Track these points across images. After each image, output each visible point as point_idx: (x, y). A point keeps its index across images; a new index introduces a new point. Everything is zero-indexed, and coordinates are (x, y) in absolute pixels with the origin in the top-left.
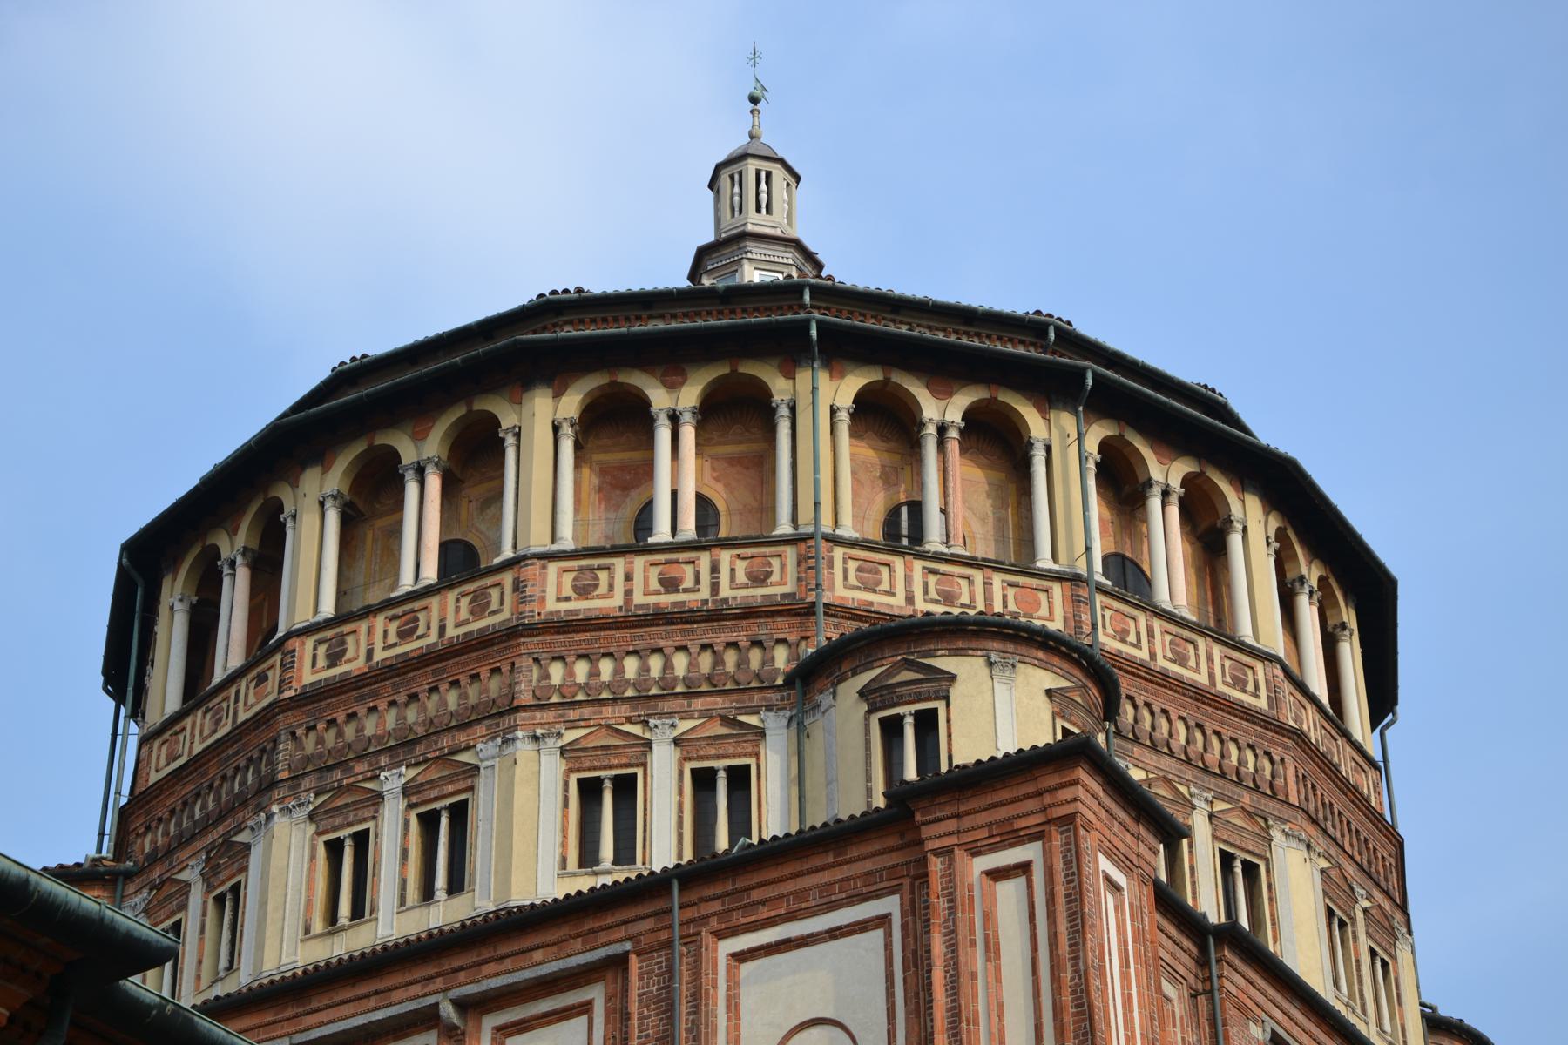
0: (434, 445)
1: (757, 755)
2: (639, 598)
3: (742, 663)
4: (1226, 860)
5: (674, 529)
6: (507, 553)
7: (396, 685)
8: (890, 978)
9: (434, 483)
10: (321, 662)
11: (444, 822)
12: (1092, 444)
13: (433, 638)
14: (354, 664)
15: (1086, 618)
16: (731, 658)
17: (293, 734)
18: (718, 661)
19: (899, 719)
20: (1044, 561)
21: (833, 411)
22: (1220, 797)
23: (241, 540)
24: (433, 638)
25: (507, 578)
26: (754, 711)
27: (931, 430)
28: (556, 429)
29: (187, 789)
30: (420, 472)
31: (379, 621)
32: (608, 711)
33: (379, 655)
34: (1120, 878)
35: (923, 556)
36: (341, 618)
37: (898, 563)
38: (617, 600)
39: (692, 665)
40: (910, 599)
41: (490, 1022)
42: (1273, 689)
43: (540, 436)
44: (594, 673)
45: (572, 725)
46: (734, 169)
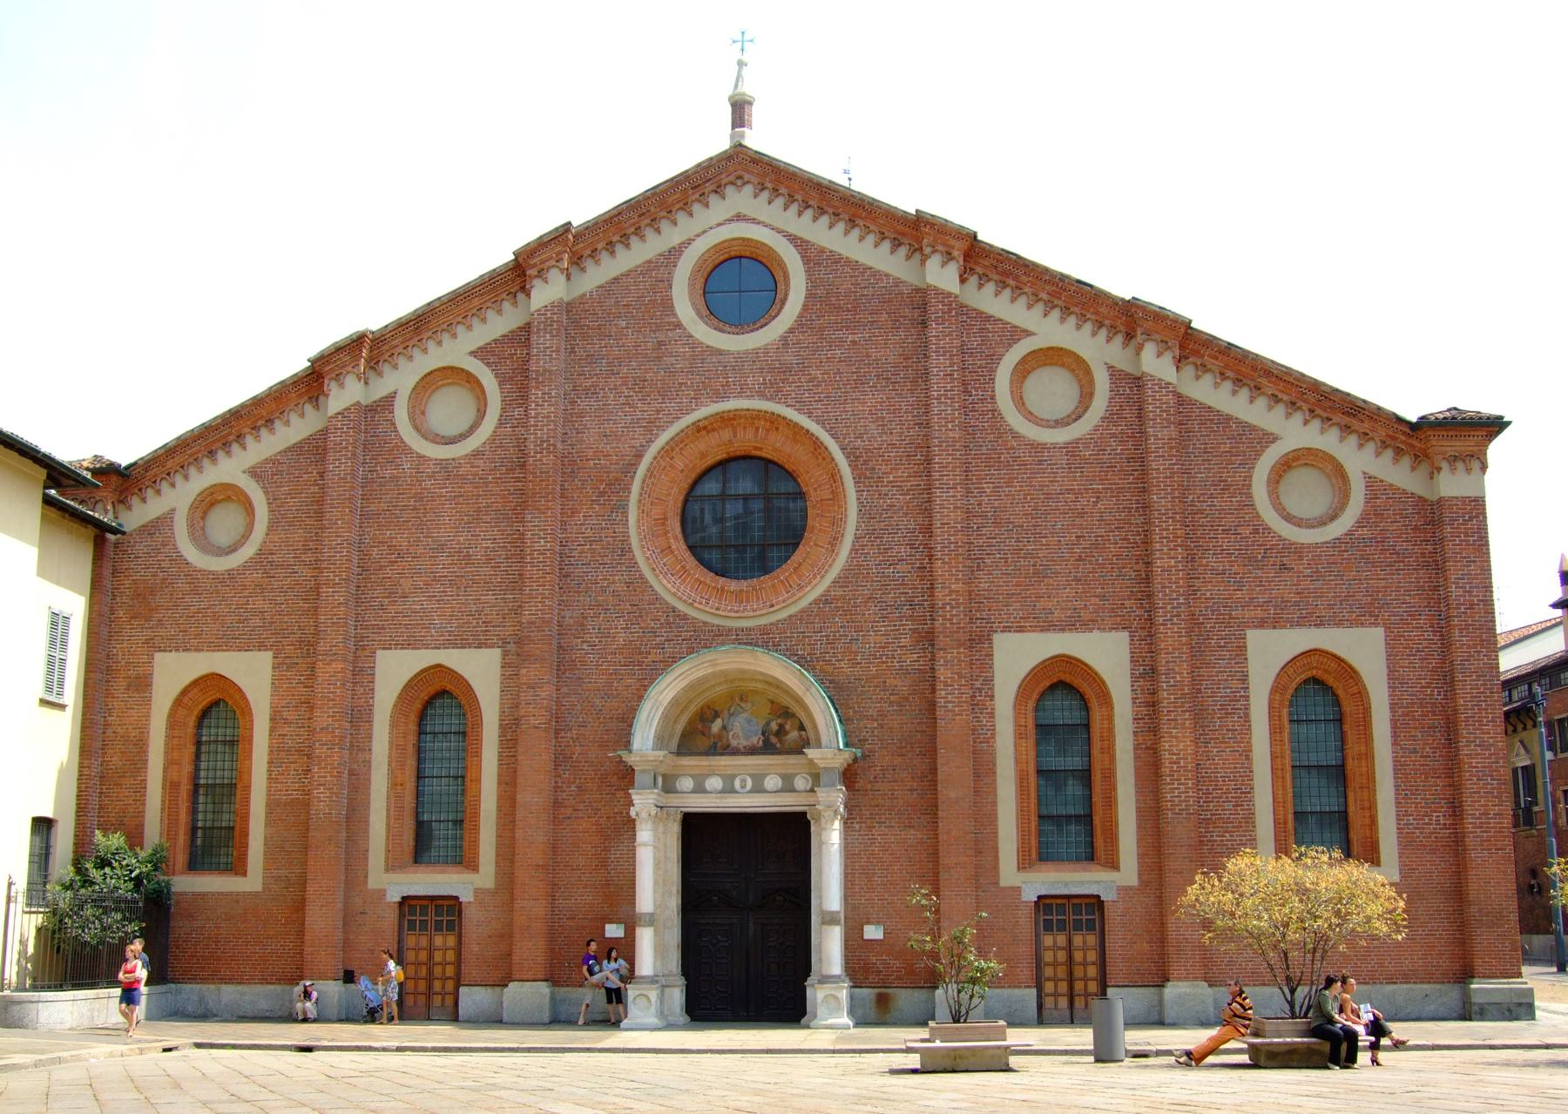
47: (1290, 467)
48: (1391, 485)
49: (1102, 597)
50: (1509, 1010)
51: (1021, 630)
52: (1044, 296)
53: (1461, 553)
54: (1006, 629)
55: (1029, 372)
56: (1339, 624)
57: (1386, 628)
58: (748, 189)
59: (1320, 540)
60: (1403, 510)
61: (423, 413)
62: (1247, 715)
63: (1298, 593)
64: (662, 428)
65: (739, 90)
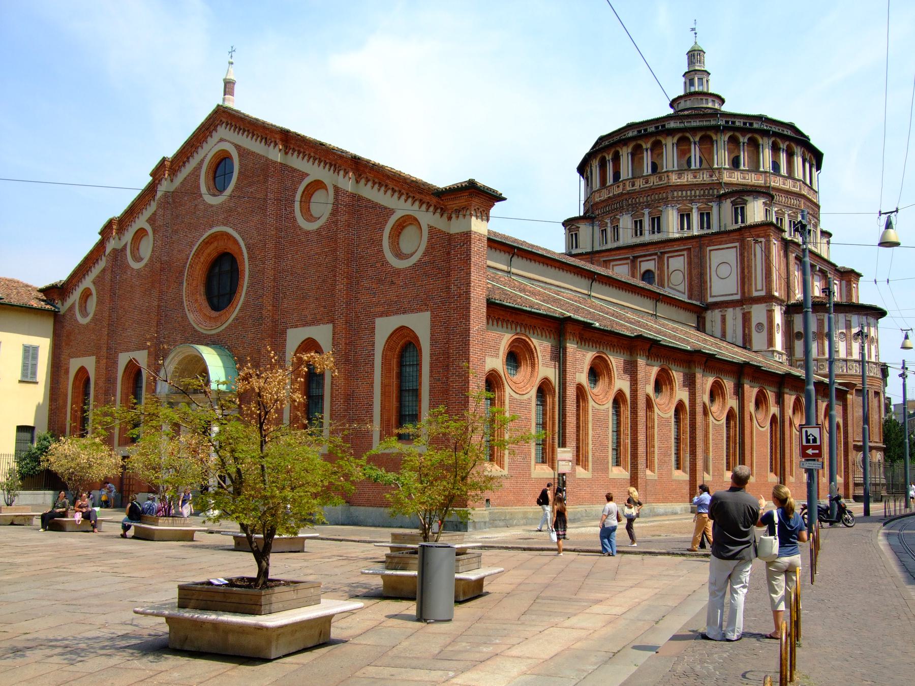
0: (649, 146)
1: (711, 210)
2: (689, 180)
3: (709, 192)
4: (790, 221)
5: (695, 166)
6: (665, 170)
7: (645, 193)
8: (737, 257)
9: (649, 152)
10: (631, 186)
11: (656, 219)
12: (770, 144)
13: (652, 184)
14: (636, 187)
15: (768, 180)
16: (706, 192)
17: (626, 200)
18: (704, 192)
19: (738, 208)
20: (762, 169)
21: (724, 142)
22: (790, 210)
23: (610, 157)
24: (652, 184)
25: (666, 175)
26: (711, 202)
27: (742, 144)
28: (673, 144)
29: (605, 204)
30: (647, 150)
31: (641, 180)
32: (685, 202)
33: (642, 186)
34: (776, 242)
35: (740, 170)
36: (633, 178)
37: (736, 173)
38: (686, 180)
39: (700, 193)
40: (738, 179)
41: (666, 255)
42: (800, 186)
43: (669, 146)
44: (682, 194)
45: (679, 204)
46: (692, 53)
47: (404, 227)
48: (439, 230)
49: (325, 307)
50: (456, 526)
51: (296, 326)
52: (312, 154)
53: (457, 266)
54: (292, 327)
55: (312, 195)
56: (412, 312)
57: (432, 311)
58: (224, 125)
59: (407, 265)
60: (442, 243)
61: (138, 249)
62: (373, 363)
63: (397, 296)
64: (194, 245)
65: (228, 77)
